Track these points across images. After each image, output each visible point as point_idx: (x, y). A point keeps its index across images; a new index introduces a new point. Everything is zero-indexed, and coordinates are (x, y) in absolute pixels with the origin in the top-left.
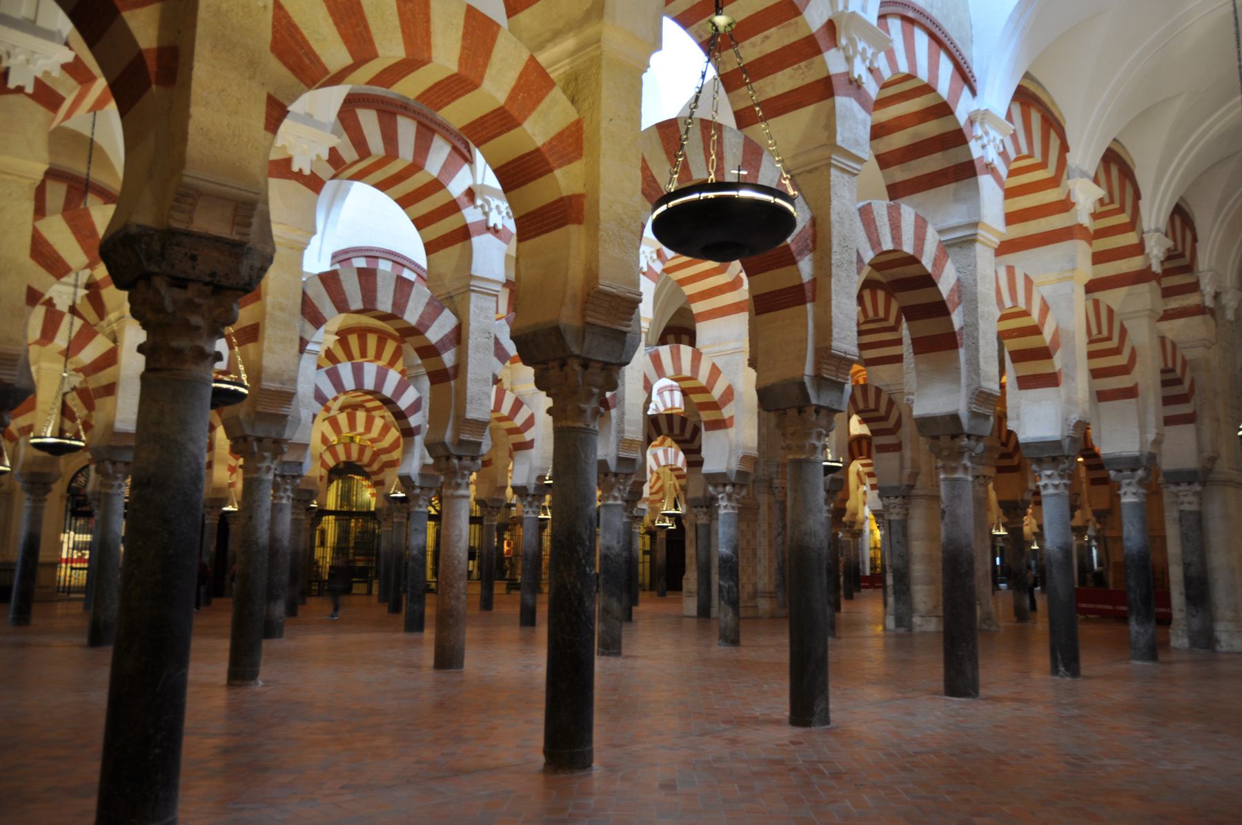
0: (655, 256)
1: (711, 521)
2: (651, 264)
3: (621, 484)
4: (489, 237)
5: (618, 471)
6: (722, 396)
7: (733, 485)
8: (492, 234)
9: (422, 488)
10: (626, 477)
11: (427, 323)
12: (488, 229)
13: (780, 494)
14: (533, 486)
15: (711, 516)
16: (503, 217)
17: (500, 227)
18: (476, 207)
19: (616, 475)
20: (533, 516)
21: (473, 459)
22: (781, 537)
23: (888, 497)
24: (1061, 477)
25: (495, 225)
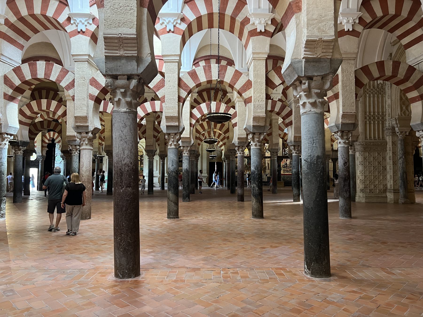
0: (179, 21)
1: (355, 153)
2: (177, 26)
3: (173, 138)
4: (80, 35)
5: (169, 132)
6: (243, 86)
7: (254, 134)
8: (81, 34)
9: (184, 147)
10: (175, 135)
11: (60, 79)
12: (79, 32)
13: (401, 136)
14: (237, 142)
15: (355, 150)
16: (86, 26)
17: (84, 30)
18: (72, 24)
19: (169, 134)
20: (240, 155)
21: (87, 133)
22: (402, 159)
23: (418, 131)
24: (308, 96)
25: (81, 30)
